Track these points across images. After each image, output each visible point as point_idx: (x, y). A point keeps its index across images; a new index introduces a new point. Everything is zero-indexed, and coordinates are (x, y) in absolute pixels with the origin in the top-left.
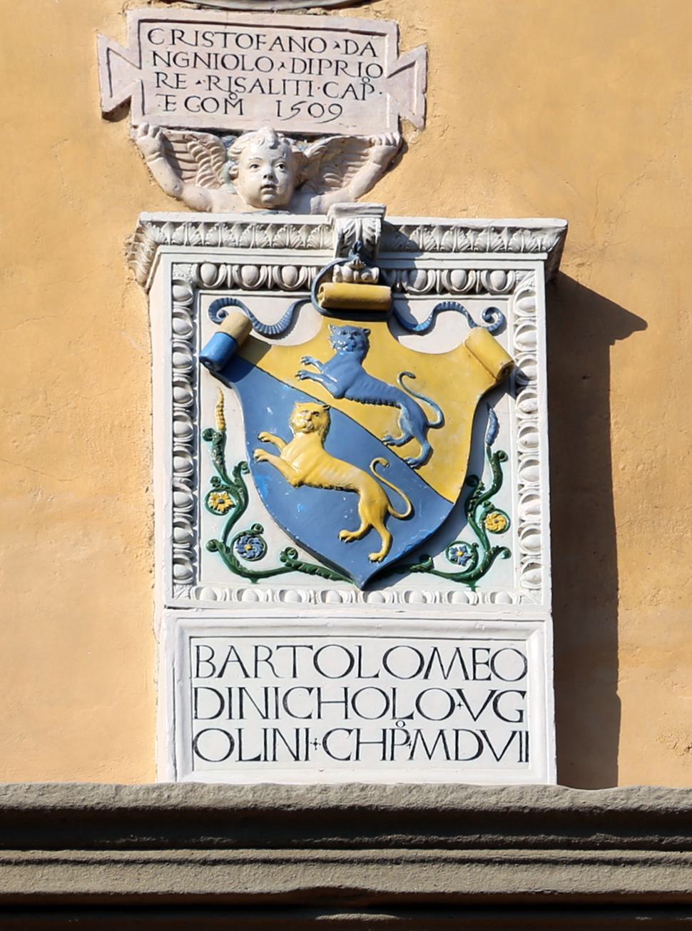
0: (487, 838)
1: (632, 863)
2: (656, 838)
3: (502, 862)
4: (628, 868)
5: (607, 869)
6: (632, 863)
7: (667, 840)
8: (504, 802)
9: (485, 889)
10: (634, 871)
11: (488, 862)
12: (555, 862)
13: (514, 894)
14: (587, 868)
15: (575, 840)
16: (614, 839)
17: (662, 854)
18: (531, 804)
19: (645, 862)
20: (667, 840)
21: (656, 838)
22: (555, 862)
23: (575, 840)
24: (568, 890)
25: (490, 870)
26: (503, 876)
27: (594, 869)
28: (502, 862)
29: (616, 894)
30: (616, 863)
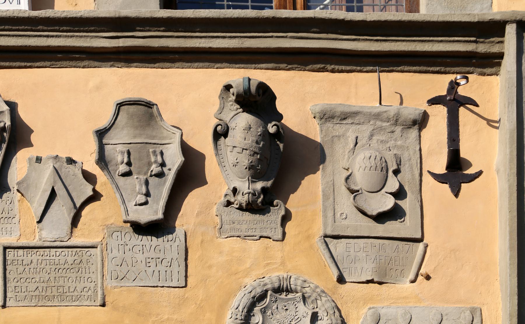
0: (7, 27)
1: (53, 36)
2: (58, 28)
3: (13, 36)
4: (52, 38)
5: (45, 38)
6: (53, 36)
7: (61, 29)
8: (8, 14)
9: (9, 44)
10: (54, 39)
11: (9, 36)
12: (29, 36)
13: (18, 46)
14: (39, 38)
15: (34, 28)
16: (45, 28)
17: (61, 34)
18: (16, 15)
19: (56, 36)
20: (61, 29)
21: (58, 28)
22: (29, 36)
23: (34, 28)
24: (34, 45)
25: (10, 39)
26: (14, 40)
27: (42, 38)
28: (13, 36)
29: (49, 47)
30: (48, 36)
